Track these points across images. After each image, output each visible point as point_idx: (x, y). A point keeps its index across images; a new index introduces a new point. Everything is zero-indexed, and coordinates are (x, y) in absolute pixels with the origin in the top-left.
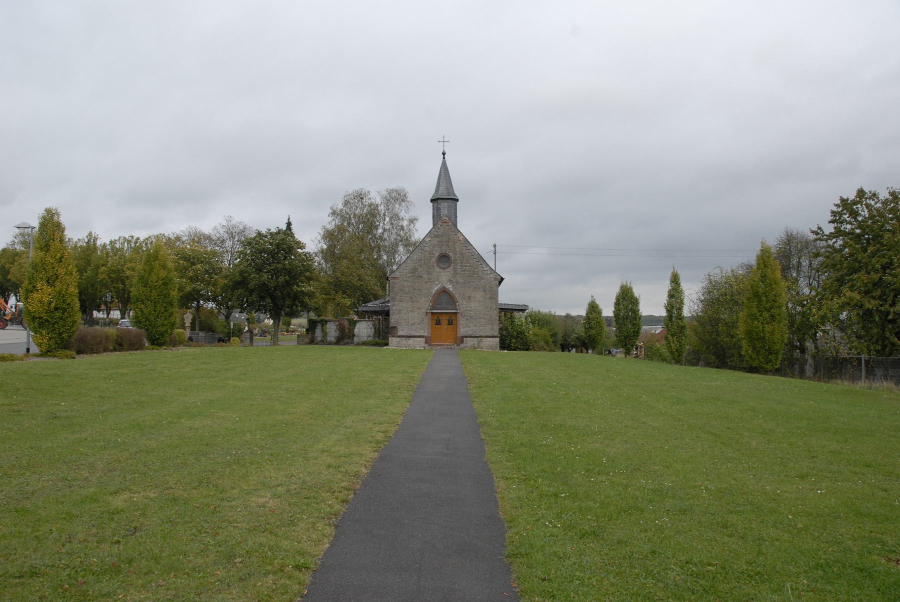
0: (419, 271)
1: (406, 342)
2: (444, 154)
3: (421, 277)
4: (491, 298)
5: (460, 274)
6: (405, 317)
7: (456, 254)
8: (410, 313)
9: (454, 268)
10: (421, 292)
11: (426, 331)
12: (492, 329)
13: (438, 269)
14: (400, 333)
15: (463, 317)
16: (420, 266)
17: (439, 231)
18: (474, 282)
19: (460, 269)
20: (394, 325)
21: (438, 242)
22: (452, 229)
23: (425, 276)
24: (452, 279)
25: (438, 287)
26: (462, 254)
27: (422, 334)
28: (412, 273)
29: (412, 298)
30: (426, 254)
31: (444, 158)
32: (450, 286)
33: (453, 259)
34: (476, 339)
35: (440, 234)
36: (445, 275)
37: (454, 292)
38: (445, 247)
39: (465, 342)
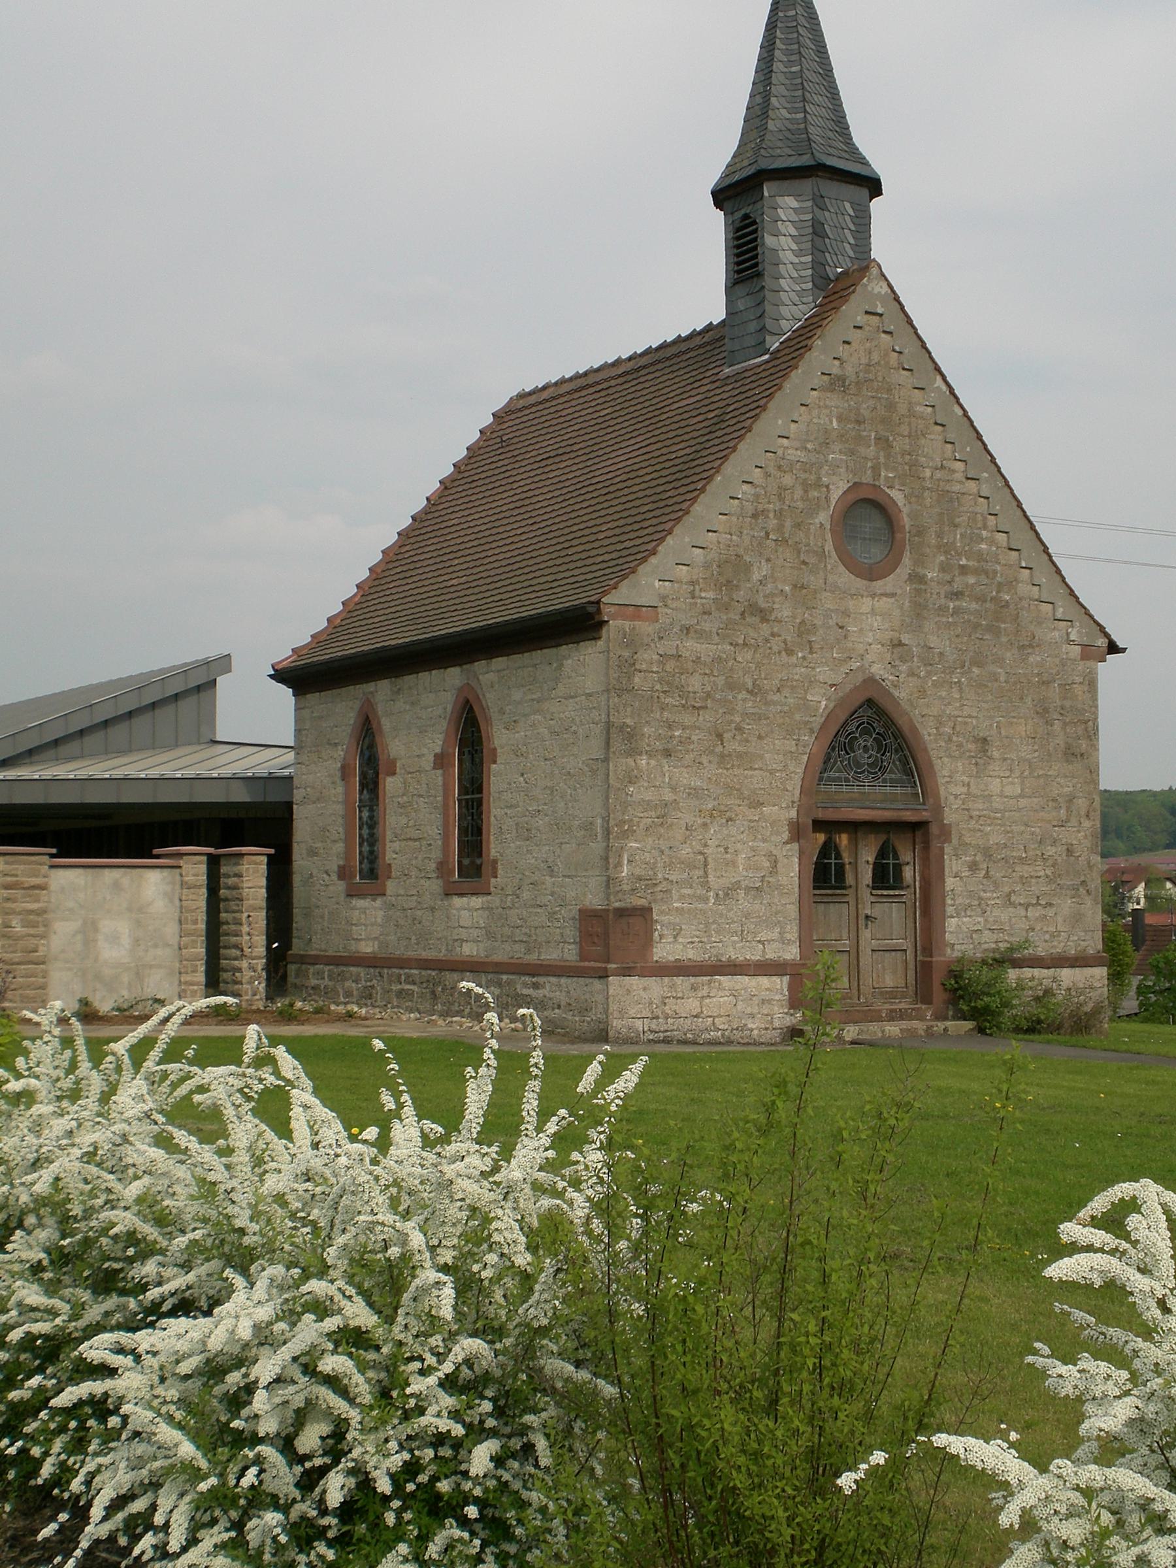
0: (756, 576)
3: (764, 615)
5: (942, 609)
6: (685, 851)
10: (767, 703)
11: (792, 932)
12: (1077, 918)
13: (844, 578)
14: (664, 951)
23: (784, 611)
24: (906, 638)
29: (720, 736)
33: (907, 522)
35: (850, 370)
36: (873, 612)
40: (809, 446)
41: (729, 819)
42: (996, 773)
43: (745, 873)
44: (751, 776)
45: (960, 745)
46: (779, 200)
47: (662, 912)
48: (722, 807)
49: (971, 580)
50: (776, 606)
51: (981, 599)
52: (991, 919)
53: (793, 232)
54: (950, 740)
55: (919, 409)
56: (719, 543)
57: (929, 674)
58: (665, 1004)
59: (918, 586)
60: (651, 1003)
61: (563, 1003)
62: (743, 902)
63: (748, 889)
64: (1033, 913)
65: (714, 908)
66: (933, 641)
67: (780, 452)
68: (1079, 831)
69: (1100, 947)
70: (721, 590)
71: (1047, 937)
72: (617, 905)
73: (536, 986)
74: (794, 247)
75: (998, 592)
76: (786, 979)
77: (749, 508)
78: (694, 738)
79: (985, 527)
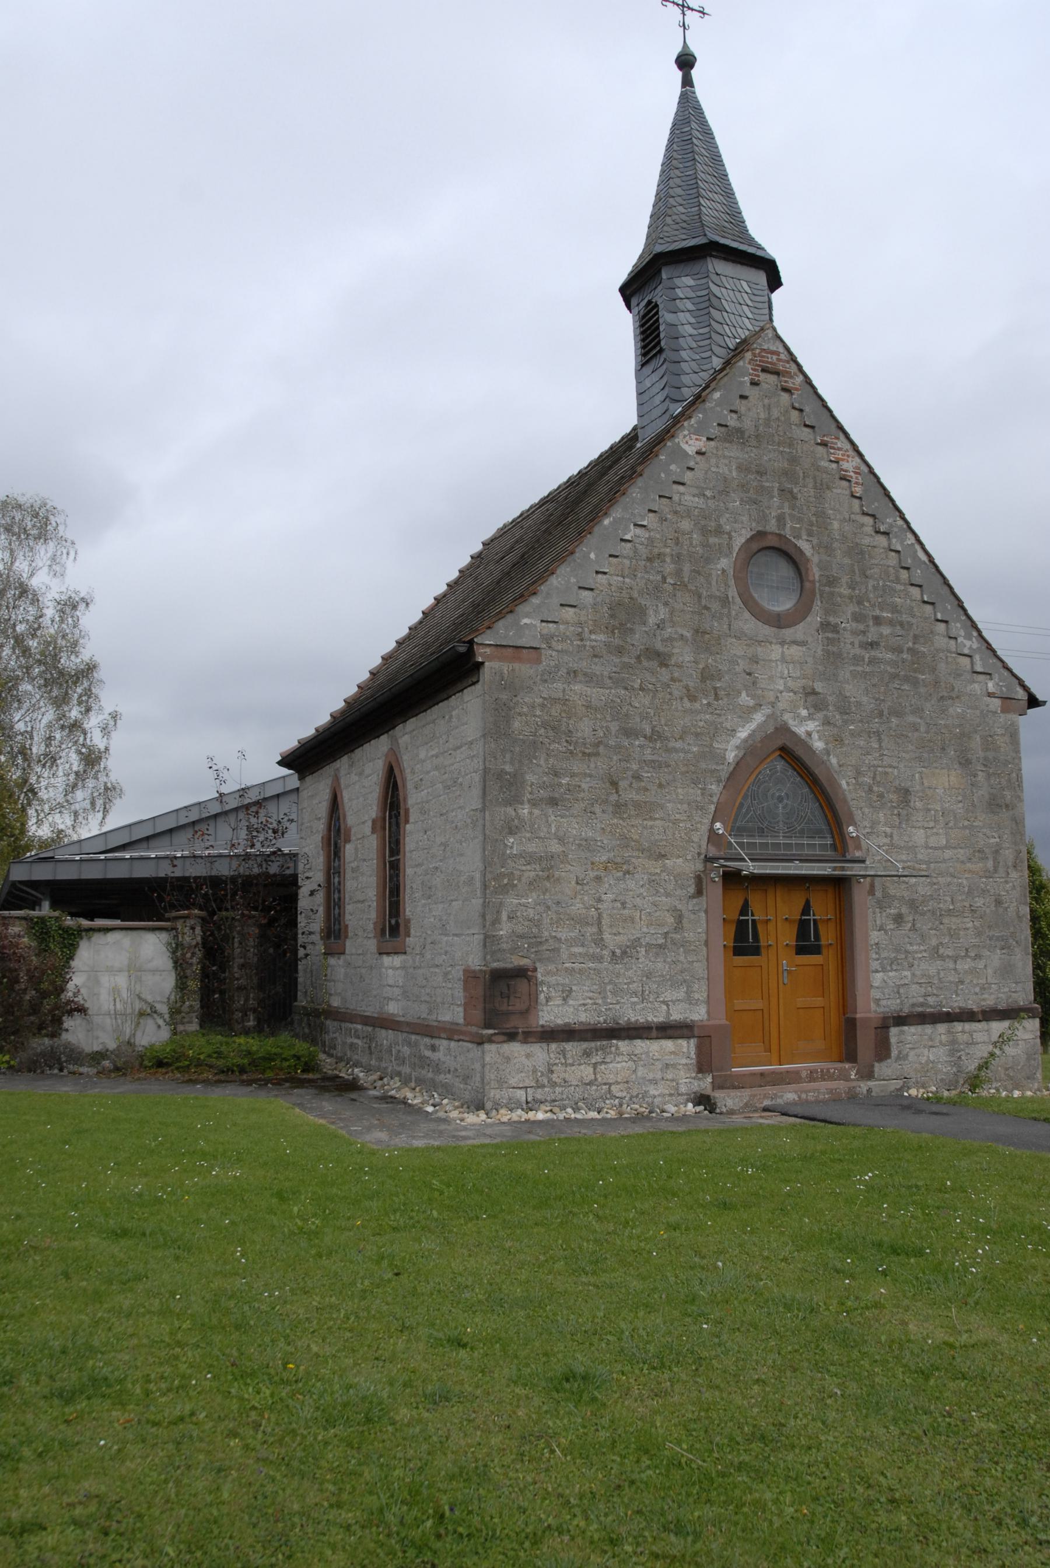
0: (652, 620)
1: (587, 1072)
2: (685, 62)
3: (662, 659)
4: (995, 804)
5: (857, 660)
6: (577, 908)
7: (829, 549)
8: (609, 880)
9: (825, 626)
10: (668, 750)
11: (700, 992)
12: (1006, 971)
13: (748, 624)
15: (881, 905)
16: (656, 591)
17: (742, 406)
18: (918, 711)
19: (854, 633)
20: (517, 961)
21: (739, 468)
22: (807, 409)
23: (683, 654)
24: (819, 687)
25: (753, 726)
26: (858, 552)
27: (677, 1015)
28: (611, 630)
29: (614, 784)
30: (686, 525)
31: (687, 82)
32: (811, 726)
34: (942, 1028)
35: (748, 424)
36: (783, 660)
37: (834, 761)
38: (775, 505)
39: (894, 1053)
40: (708, 493)
41: (628, 872)
42: (920, 824)
43: (645, 930)
44: (651, 827)
45: (881, 796)
46: (677, 281)
47: (548, 973)
48: (619, 860)
49: (886, 630)
50: (676, 651)
51: (898, 650)
52: (918, 973)
53: (691, 307)
54: (871, 790)
55: (824, 464)
56: (610, 585)
57: (846, 722)
58: (552, 1072)
59: (830, 635)
60: (535, 1071)
61: (452, 1069)
62: (644, 961)
63: (649, 946)
64: (964, 965)
65: (610, 967)
66: (850, 689)
67: (676, 498)
68: (1006, 882)
69: (1032, 997)
70: (613, 632)
71: (977, 990)
72: (495, 965)
73: (433, 1048)
74: (693, 320)
75: (914, 643)
76: (693, 1042)
77: (643, 551)
78: (584, 786)
79: (898, 580)
